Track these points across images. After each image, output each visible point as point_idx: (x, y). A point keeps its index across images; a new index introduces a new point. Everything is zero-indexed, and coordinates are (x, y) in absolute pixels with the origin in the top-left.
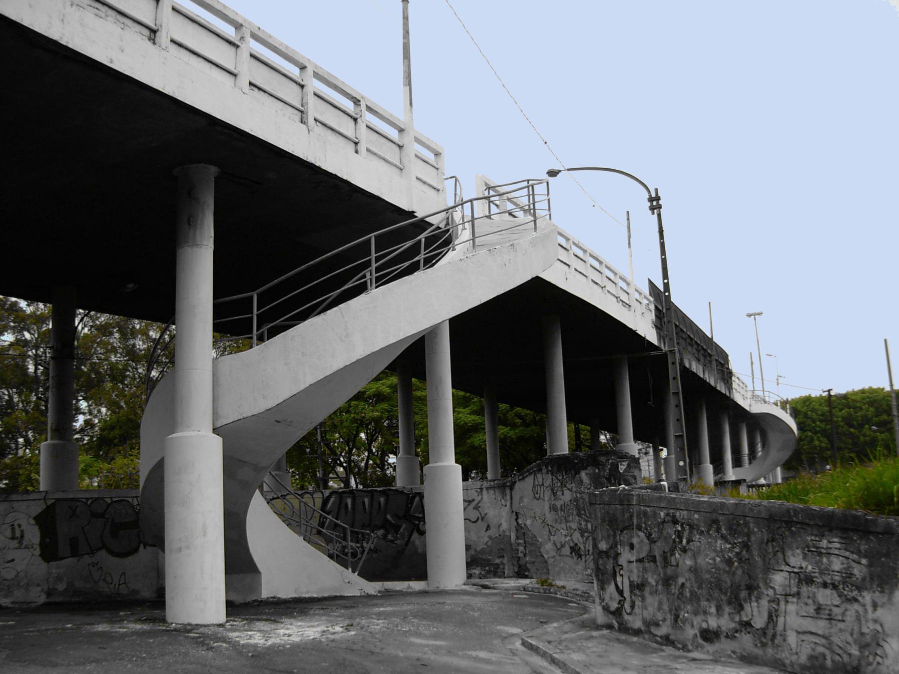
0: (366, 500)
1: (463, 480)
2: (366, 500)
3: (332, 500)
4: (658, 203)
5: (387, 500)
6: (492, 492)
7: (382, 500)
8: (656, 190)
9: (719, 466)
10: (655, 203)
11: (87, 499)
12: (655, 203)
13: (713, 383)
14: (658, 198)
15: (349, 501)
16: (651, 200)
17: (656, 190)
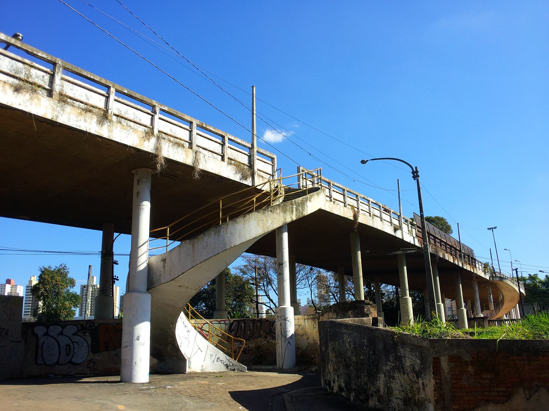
0: (251, 324)
1: (295, 314)
2: (251, 324)
3: (235, 324)
4: (417, 174)
5: (245, 324)
6: (310, 321)
7: (258, 324)
8: (416, 168)
9: (472, 308)
10: (415, 174)
11: (114, 323)
12: (415, 174)
13: (461, 265)
14: (417, 172)
15: (243, 325)
16: (413, 172)
17: (416, 168)
